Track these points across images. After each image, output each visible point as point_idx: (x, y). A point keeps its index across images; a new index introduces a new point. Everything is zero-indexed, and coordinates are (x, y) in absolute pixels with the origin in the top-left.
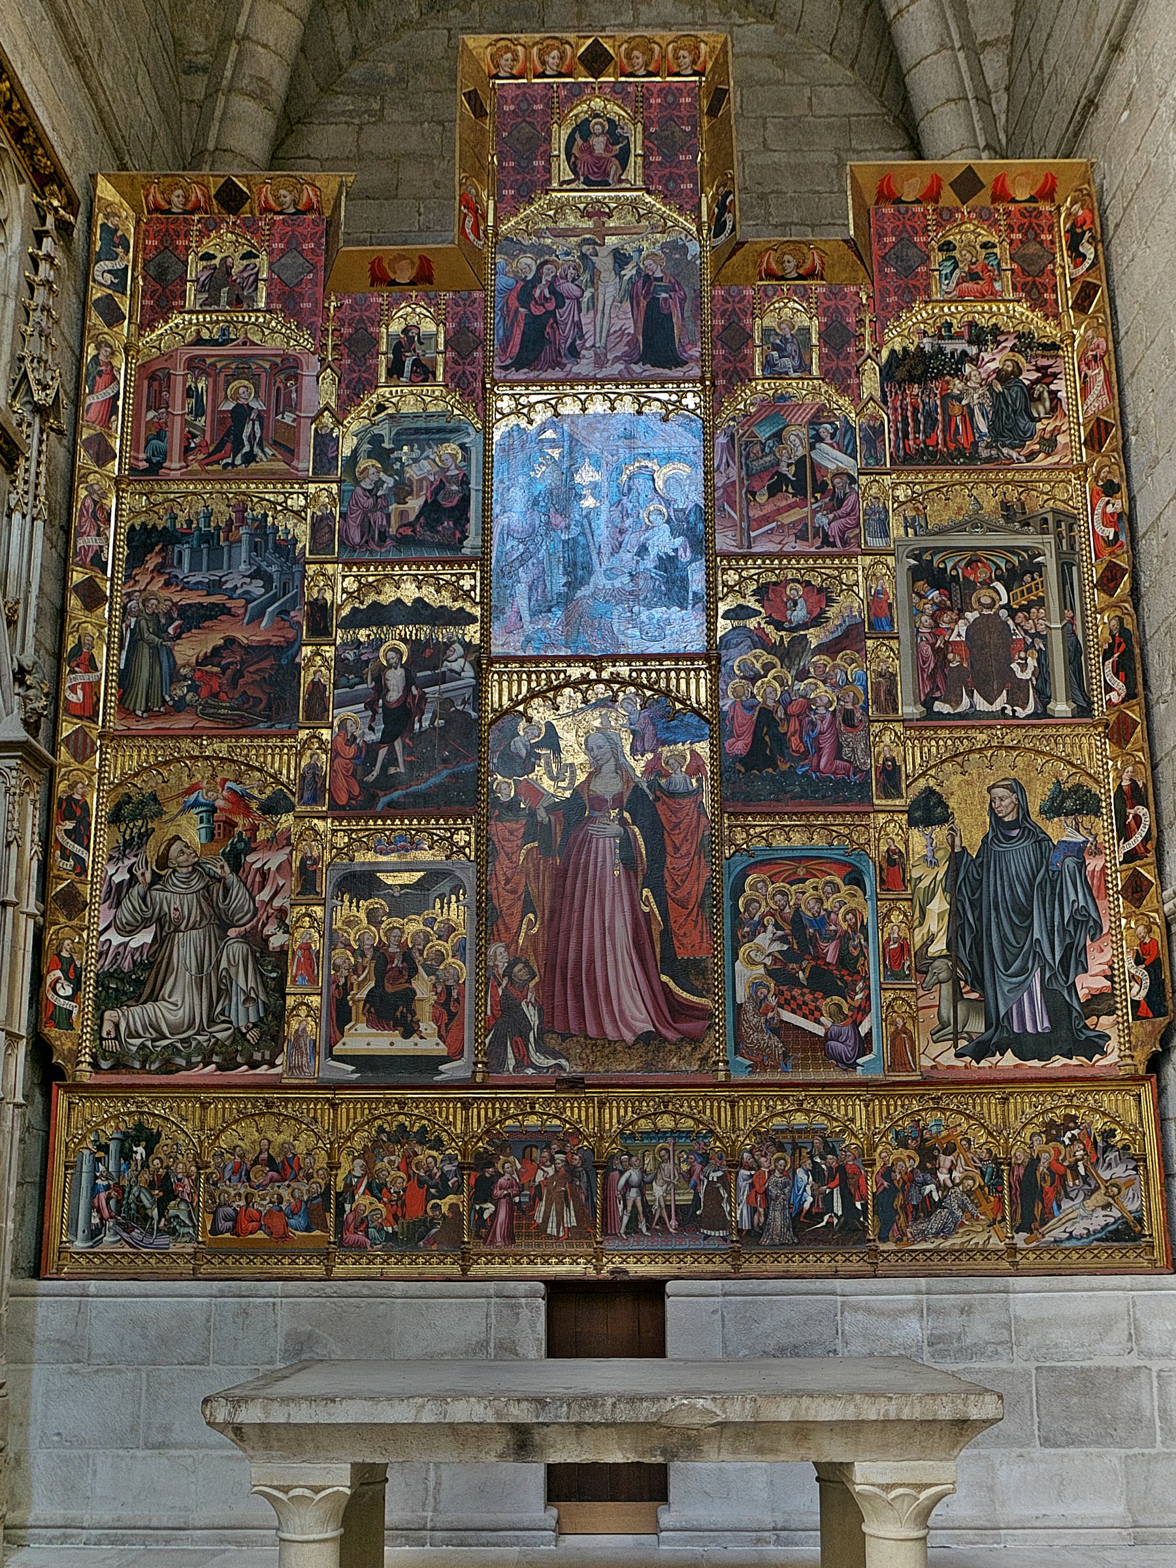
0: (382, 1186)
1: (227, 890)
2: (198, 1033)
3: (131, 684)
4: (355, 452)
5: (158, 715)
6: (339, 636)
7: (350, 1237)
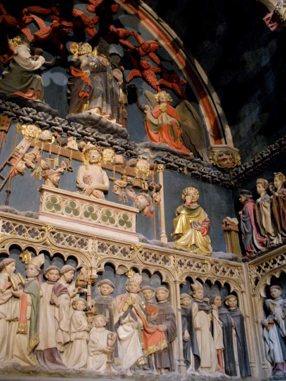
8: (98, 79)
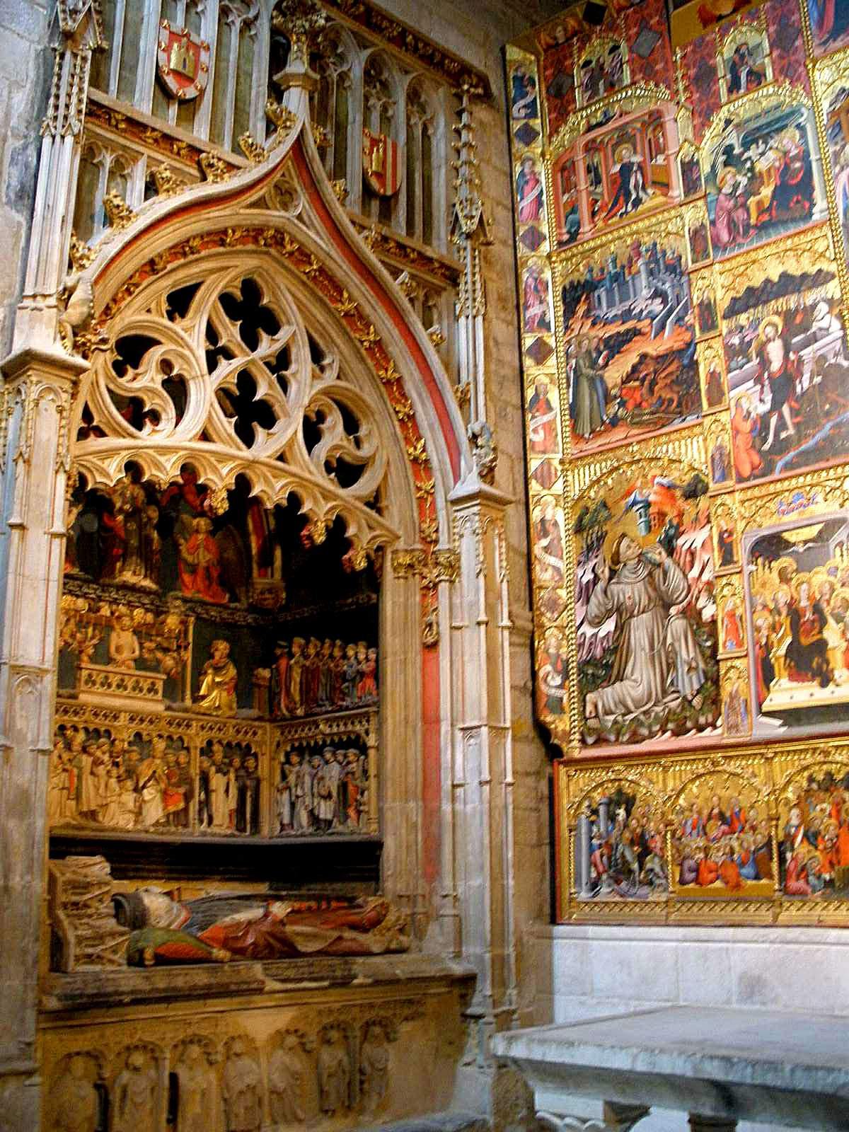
0: (817, 834)
1: (665, 573)
2: (655, 705)
3: (578, 415)
4: (713, 167)
5: (600, 434)
6: (724, 326)
7: (794, 884)
8: (132, 526)
